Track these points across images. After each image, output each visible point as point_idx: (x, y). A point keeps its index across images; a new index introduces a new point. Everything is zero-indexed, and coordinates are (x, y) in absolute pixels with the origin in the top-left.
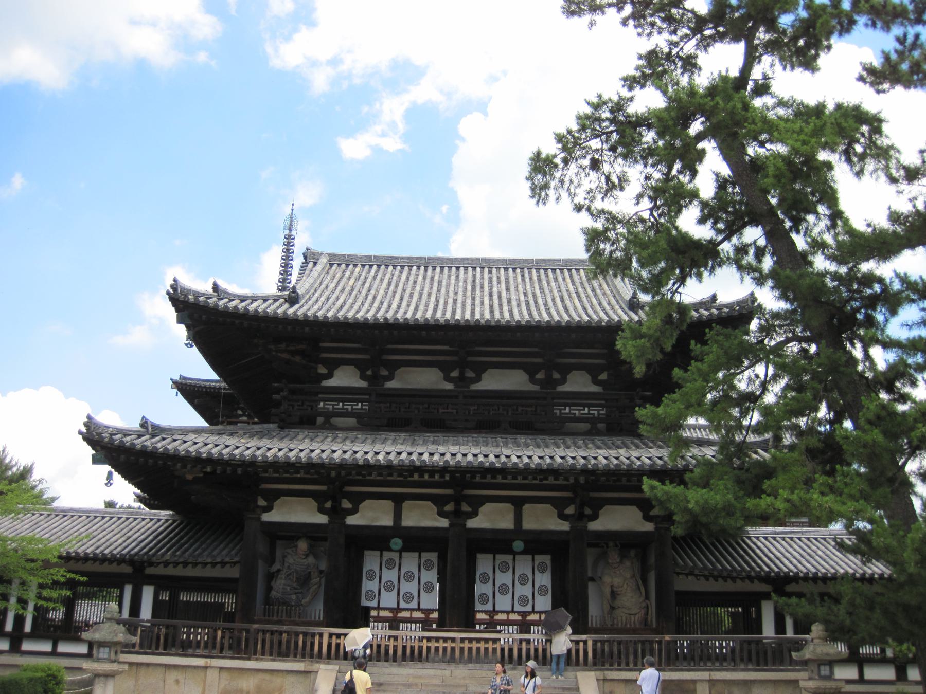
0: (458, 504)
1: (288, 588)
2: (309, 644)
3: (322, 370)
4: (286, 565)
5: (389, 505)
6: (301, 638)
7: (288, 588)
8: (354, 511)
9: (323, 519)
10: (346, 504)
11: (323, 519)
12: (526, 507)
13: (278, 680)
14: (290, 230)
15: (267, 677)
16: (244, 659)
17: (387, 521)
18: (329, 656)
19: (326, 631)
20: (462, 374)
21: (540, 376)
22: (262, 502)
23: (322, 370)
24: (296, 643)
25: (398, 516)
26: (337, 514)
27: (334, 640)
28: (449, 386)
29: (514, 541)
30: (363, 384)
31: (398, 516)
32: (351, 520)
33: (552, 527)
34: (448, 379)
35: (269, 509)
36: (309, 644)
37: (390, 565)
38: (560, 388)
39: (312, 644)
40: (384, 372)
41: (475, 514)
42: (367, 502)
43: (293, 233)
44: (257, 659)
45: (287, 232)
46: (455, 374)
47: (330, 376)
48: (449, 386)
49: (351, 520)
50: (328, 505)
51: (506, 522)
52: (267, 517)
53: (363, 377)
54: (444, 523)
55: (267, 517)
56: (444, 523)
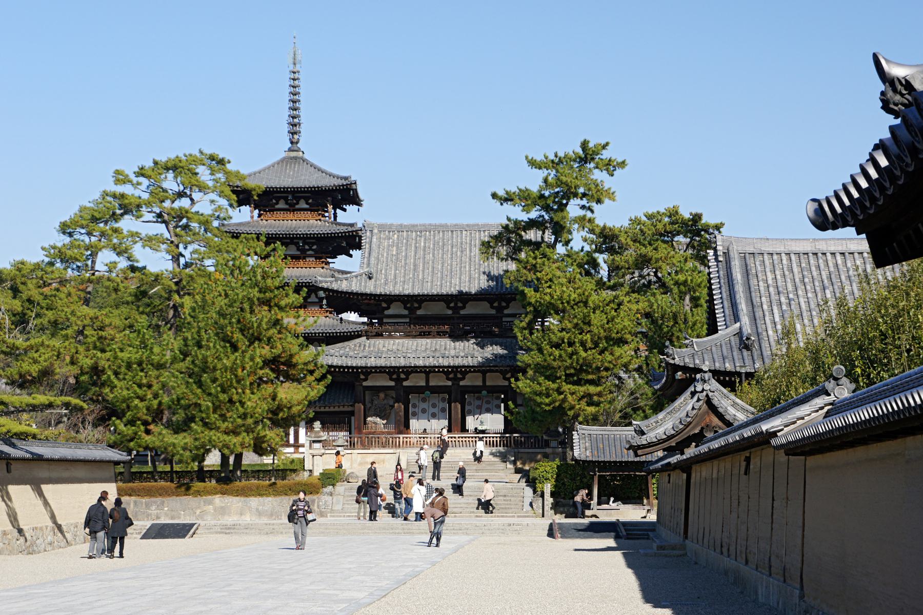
0: (455, 375)
3: (384, 305)
5: (424, 375)
8: (407, 379)
9: (392, 384)
10: (403, 376)
11: (392, 384)
12: (488, 374)
13: (382, 456)
14: (295, 64)
17: (423, 384)
19: (401, 436)
20: (456, 304)
21: (496, 304)
23: (384, 305)
25: (427, 381)
26: (399, 381)
28: (450, 312)
30: (406, 312)
31: (427, 381)
32: (405, 384)
34: (449, 308)
35: (366, 380)
37: (424, 400)
38: (506, 312)
40: (416, 305)
41: (463, 379)
42: (413, 375)
43: (298, 68)
45: (291, 68)
46: (452, 305)
47: (388, 308)
48: (450, 312)
49: (405, 384)
50: (395, 376)
51: (479, 383)
52: (365, 384)
53: (405, 308)
54: (449, 383)
55: (365, 384)
56: (449, 383)
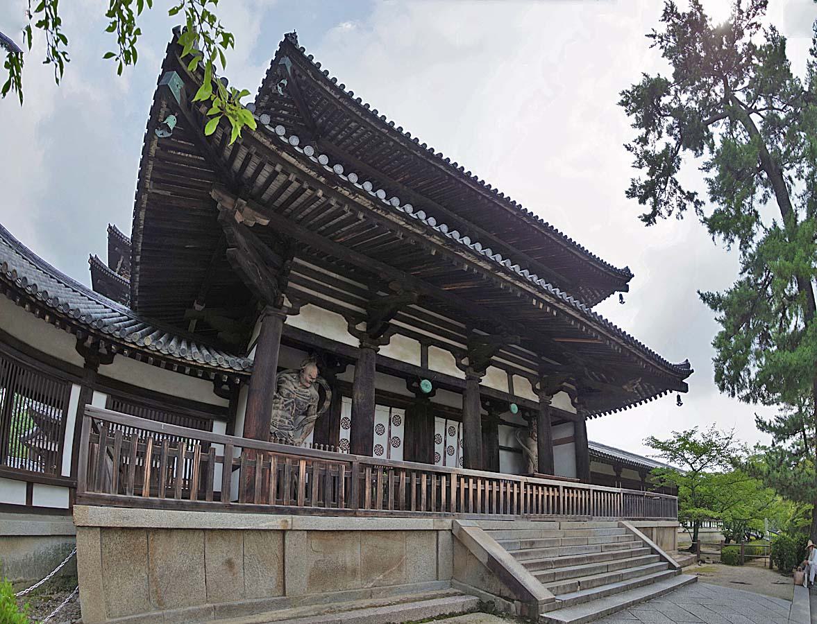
1: (287, 421)
2: (434, 489)
4: (285, 392)
6: (424, 477)
7: (287, 421)
15: (379, 541)
16: (345, 513)
18: (458, 510)
22: (287, 303)
24: (419, 486)
27: (464, 485)
29: (511, 403)
31: (424, 359)
33: (530, 399)
35: (295, 312)
36: (434, 489)
39: (439, 488)
44: (366, 514)
